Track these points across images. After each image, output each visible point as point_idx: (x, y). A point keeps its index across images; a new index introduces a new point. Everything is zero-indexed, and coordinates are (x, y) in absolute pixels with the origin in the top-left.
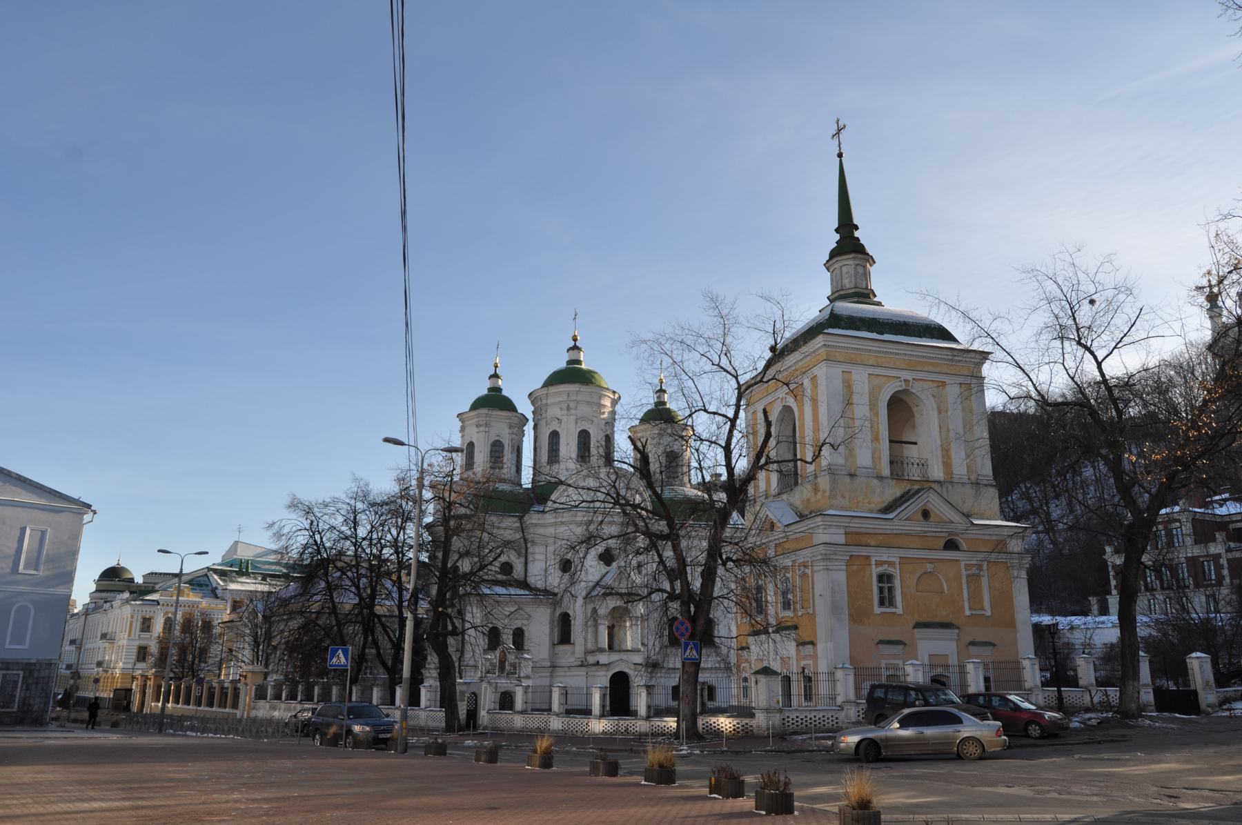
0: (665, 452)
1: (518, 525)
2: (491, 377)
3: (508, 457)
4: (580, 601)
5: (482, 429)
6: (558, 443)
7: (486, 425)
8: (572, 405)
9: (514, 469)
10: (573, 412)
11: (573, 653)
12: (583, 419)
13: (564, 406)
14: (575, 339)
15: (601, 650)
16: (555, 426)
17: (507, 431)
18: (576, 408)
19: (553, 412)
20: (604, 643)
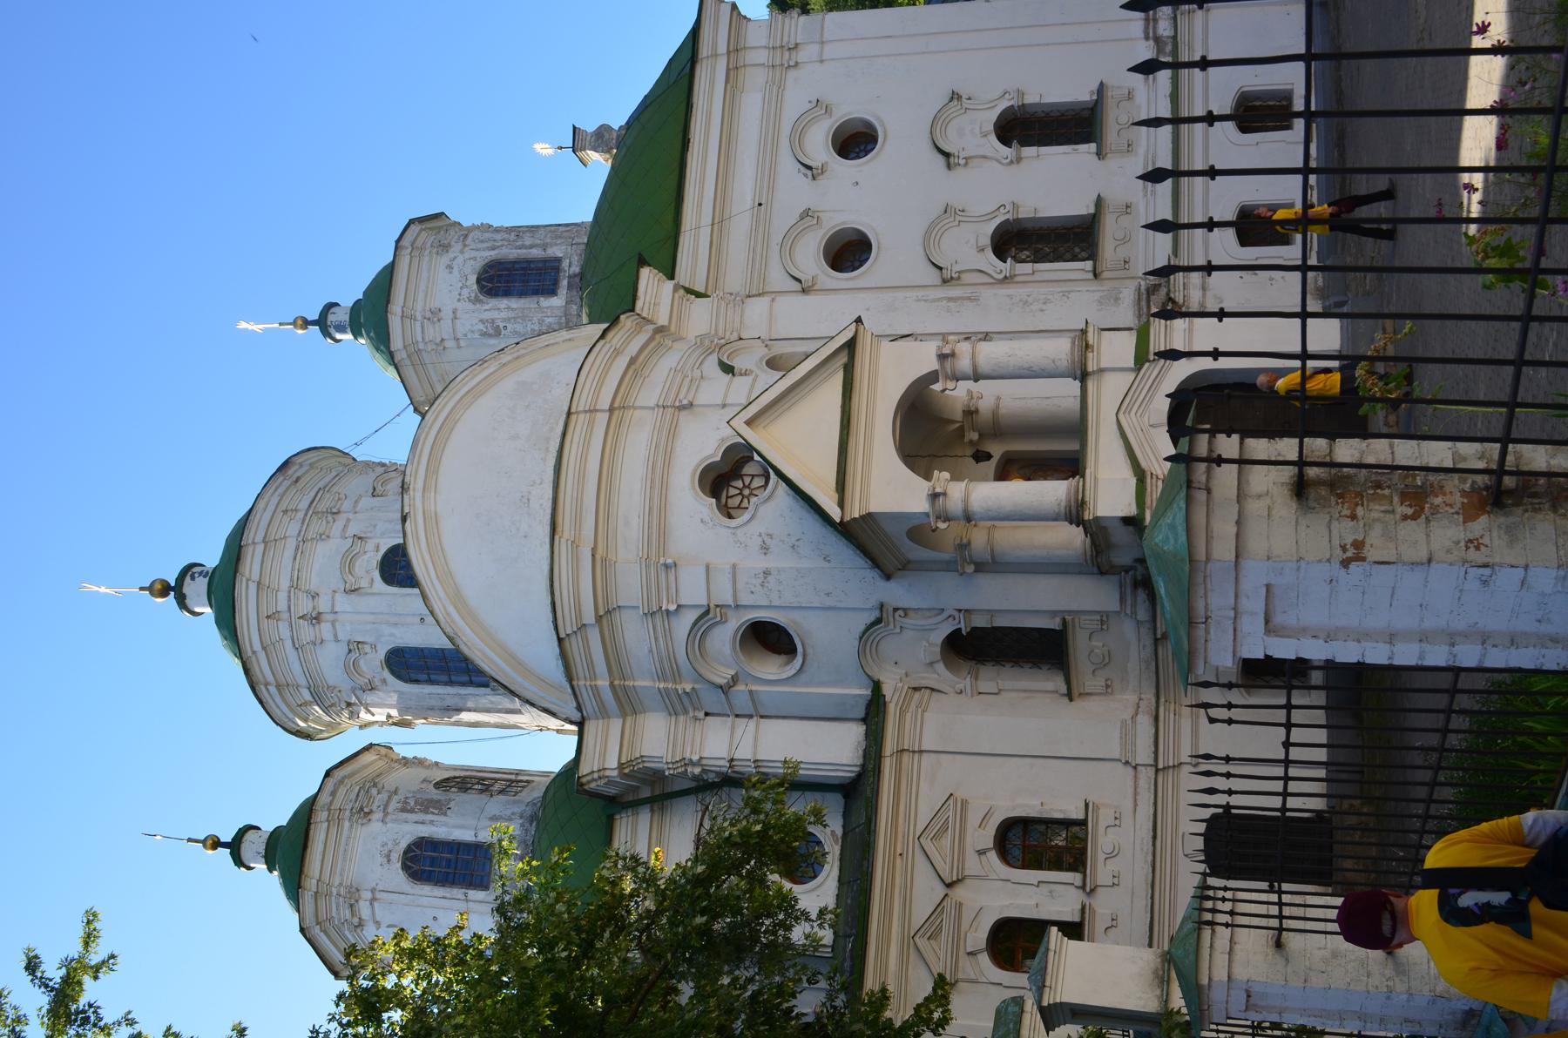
0: (476, 301)
1: (644, 817)
2: (239, 861)
3: (459, 825)
4: (896, 593)
5: (364, 909)
6: (419, 652)
7: (352, 896)
8: (304, 606)
9: (496, 805)
10: (323, 605)
11: (1104, 618)
12: (348, 562)
13: (307, 632)
14: (163, 589)
15: (1075, 513)
16: (373, 663)
17: (375, 826)
18: (315, 596)
19: (330, 662)
20: (1052, 492)
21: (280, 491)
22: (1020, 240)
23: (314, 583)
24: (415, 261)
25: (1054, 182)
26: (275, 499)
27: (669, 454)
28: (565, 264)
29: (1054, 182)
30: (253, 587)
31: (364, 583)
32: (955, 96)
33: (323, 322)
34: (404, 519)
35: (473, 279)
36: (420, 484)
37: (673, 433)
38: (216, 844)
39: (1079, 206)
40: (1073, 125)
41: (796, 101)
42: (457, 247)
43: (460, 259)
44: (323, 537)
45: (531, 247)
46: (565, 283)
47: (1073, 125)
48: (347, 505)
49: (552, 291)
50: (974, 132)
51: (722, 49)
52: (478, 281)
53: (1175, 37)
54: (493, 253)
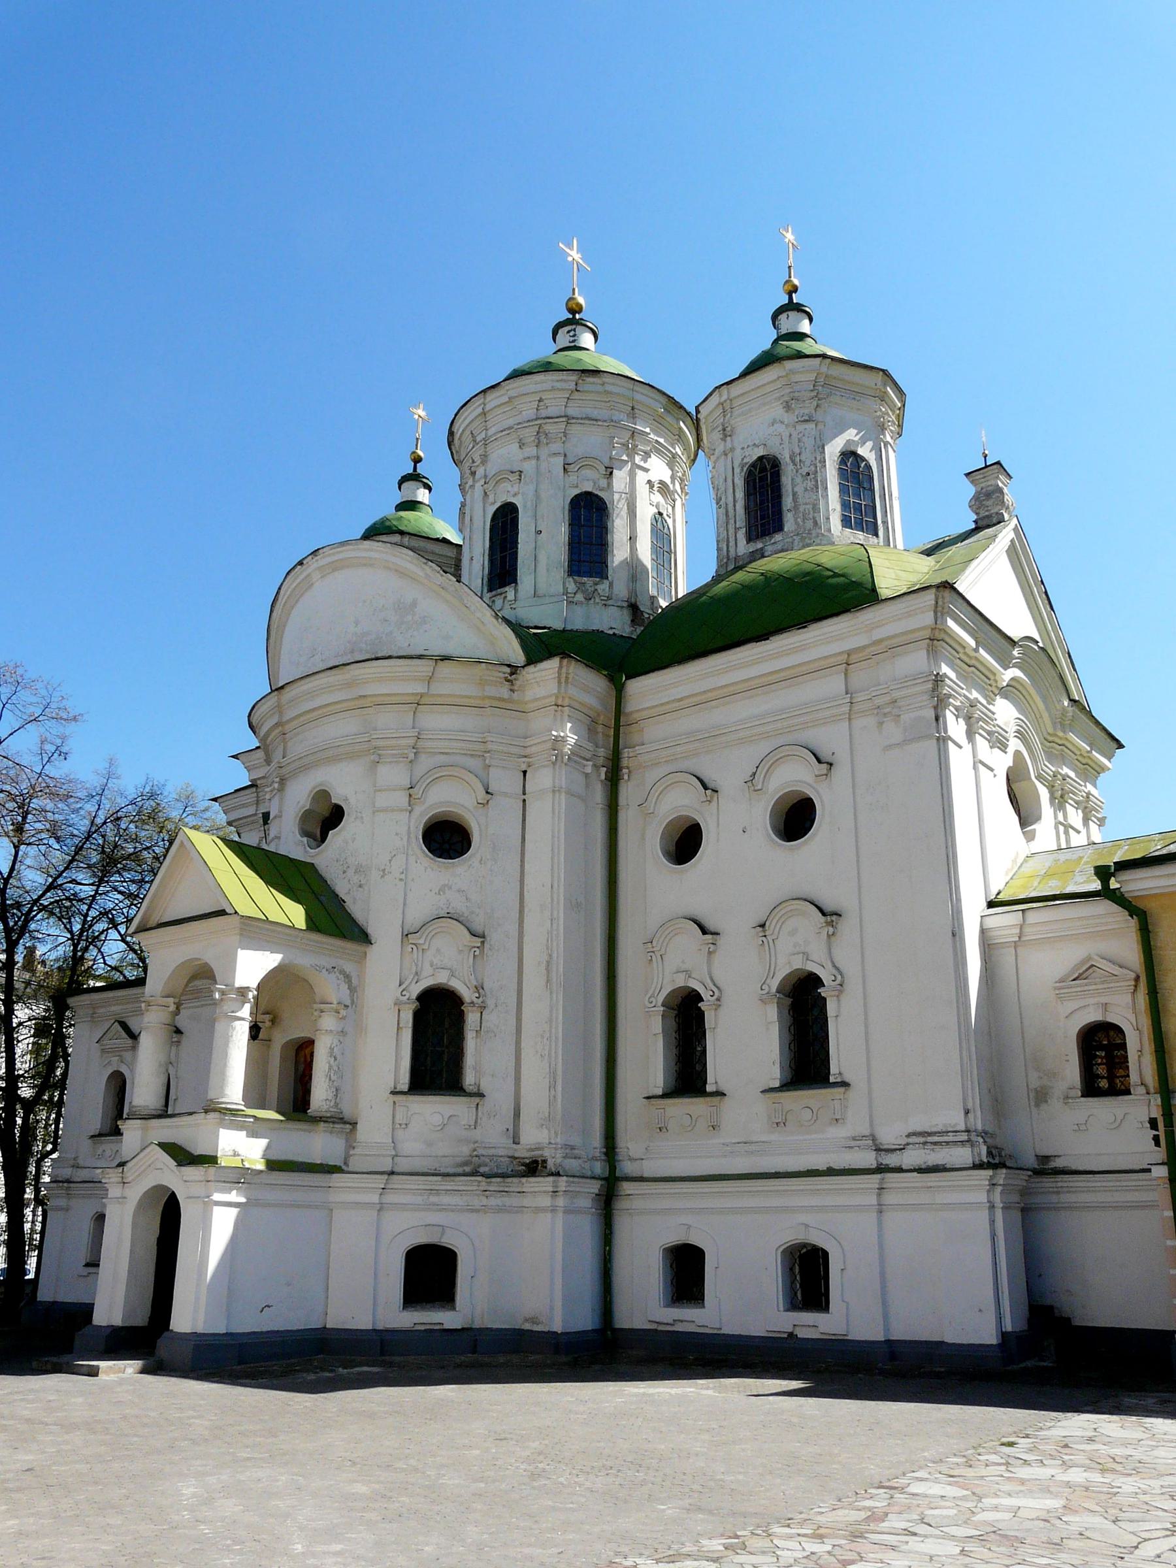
21: (558, 385)
22: (687, 1016)
23: (493, 457)
24: (778, 384)
25: (748, 1043)
26: (547, 386)
27: (335, 759)
28: (778, 537)
29: (748, 1043)
30: (480, 410)
31: (491, 498)
32: (830, 915)
33: (792, 307)
34: (301, 563)
35: (761, 452)
36: (321, 563)
37: (351, 756)
38: (417, 460)
39: (717, 1070)
40: (807, 1060)
41: (831, 739)
42: (789, 418)
43: (780, 428)
44: (522, 445)
45: (794, 494)
46: (759, 545)
47: (807, 1060)
48: (556, 447)
49: (749, 540)
50: (799, 947)
51: (878, 634)
52: (761, 458)
53: (899, 1170)
54: (788, 459)
